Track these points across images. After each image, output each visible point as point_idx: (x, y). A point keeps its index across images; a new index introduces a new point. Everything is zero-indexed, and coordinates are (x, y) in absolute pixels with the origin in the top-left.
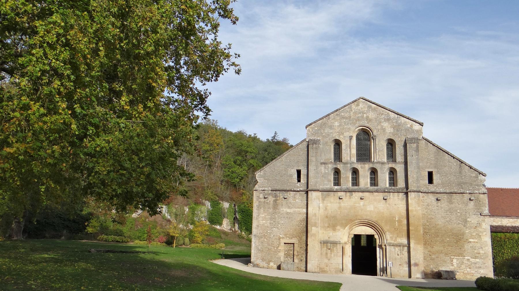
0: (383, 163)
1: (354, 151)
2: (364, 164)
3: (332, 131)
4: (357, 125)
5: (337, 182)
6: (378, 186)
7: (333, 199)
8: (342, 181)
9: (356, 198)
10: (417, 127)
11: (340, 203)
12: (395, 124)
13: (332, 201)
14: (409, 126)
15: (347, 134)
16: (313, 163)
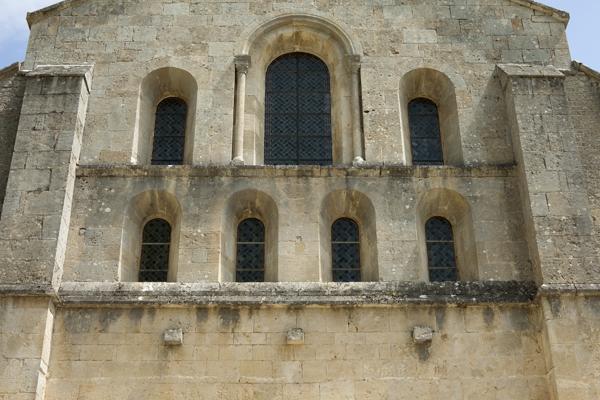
0: (397, 172)
1: (252, 124)
2: (301, 175)
3: (151, 36)
4: (271, 16)
5: (154, 260)
6: (374, 278)
7: (125, 342)
8: (181, 255)
9: (260, 339)
10: (539, 28)
11: (162, 369)
12: (444, 15)
13: (123, 358)
14: (505, 22)
15: (223, 53)
16: (34, 160)
